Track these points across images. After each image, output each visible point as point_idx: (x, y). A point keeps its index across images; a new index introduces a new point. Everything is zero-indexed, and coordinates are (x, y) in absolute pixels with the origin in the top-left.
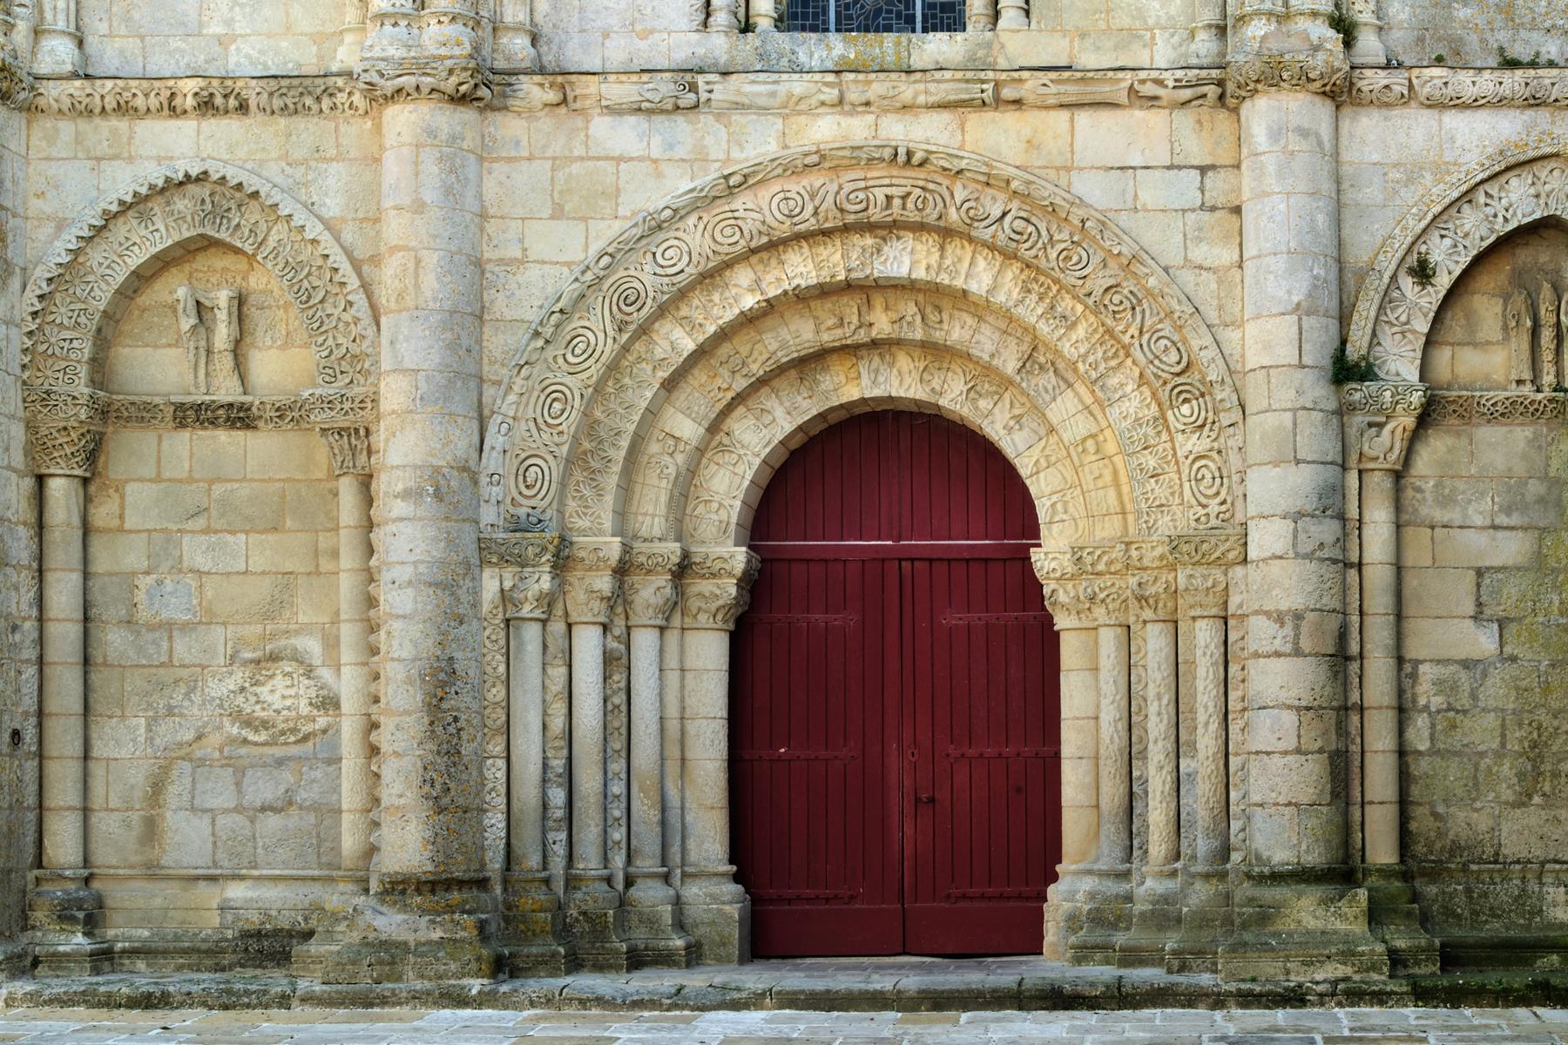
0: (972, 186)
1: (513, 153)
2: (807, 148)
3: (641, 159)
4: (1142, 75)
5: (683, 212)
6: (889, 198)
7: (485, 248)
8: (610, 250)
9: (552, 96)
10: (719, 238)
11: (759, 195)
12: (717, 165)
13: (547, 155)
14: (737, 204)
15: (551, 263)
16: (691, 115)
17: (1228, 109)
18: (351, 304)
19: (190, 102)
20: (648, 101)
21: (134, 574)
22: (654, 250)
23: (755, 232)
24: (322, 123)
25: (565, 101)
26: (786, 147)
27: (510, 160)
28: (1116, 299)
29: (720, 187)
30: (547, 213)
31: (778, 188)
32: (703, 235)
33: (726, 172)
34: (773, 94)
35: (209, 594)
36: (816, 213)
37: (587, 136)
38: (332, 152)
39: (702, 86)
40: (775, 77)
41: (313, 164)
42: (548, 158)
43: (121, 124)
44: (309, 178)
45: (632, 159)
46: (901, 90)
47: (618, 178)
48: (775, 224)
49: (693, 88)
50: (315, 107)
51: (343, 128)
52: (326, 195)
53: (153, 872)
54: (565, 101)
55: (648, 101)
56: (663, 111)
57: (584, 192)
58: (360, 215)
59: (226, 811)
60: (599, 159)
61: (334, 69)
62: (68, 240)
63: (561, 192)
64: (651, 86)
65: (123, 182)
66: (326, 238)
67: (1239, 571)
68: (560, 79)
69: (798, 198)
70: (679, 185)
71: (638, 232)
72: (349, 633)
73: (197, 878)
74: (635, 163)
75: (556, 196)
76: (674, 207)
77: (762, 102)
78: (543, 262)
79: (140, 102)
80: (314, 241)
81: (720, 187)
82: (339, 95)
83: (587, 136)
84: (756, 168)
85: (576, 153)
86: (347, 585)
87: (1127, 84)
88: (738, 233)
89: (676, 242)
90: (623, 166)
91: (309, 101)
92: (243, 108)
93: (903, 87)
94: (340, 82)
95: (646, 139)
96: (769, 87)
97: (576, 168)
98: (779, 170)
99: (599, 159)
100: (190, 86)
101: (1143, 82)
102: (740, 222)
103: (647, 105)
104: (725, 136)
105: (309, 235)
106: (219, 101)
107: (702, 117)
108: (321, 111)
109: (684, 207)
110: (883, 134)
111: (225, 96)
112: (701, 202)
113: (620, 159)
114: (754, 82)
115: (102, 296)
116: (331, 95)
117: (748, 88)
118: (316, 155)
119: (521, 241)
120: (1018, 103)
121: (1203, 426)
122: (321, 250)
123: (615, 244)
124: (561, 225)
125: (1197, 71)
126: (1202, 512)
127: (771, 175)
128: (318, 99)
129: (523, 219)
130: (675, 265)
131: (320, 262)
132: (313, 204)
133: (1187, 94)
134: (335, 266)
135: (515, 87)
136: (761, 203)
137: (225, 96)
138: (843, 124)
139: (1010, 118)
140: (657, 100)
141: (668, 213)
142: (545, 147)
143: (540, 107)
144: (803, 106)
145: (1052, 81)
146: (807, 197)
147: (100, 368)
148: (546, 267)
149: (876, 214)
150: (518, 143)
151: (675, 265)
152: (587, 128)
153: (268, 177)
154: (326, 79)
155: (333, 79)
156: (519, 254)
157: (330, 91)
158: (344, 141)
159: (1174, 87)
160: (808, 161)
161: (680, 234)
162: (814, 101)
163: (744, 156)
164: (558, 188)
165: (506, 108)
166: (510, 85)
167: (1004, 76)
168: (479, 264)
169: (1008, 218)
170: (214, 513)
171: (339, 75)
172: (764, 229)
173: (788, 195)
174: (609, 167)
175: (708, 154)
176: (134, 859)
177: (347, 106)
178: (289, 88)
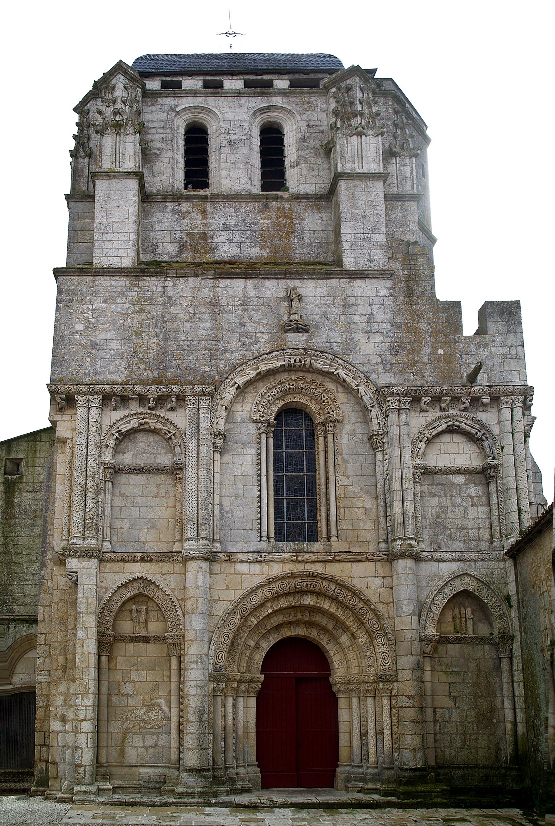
0: (327, 582)
3: (248, 574)
6: (307, 584)
9: (227, 558)
16: (260, 564)
18: (177, 611)
19: (139, 558)
21: (119, 681)
25: (229, 560)
26: (283, 572)
27: (216, 574)
28: (363, 611)
35: (137, 687)
43: (122, 564)
49: (261, 556)
51: (175, 565)
53: (122, 765)
54: (229, 560)
59: (140, 747)
62: (109, 594)
65: (122, 579)
67: (395, 684)
70: (257, 581)
72: (174, 699)
73: (133, 766)
77: (277, 560)
79: (127, 558)
86: (174, 686)
92: (151, 560)
94: (175, 554)
97: (231, 576)
100: (140, 555)
106: (146, 558)
110: (306, 568)
111: (148, 557)
112: (262, 586)
115: (116, 608)
121: (383, 645)
126: (384, 667)
128: (170, 558)
137: (148, 557)
142: (224, 571)
147: (114, 626)
149: (304, 589)
153: (157, 579)
160: (289, 575)
169: (336, 590)
170: (139, 665)
176: (117, 761)
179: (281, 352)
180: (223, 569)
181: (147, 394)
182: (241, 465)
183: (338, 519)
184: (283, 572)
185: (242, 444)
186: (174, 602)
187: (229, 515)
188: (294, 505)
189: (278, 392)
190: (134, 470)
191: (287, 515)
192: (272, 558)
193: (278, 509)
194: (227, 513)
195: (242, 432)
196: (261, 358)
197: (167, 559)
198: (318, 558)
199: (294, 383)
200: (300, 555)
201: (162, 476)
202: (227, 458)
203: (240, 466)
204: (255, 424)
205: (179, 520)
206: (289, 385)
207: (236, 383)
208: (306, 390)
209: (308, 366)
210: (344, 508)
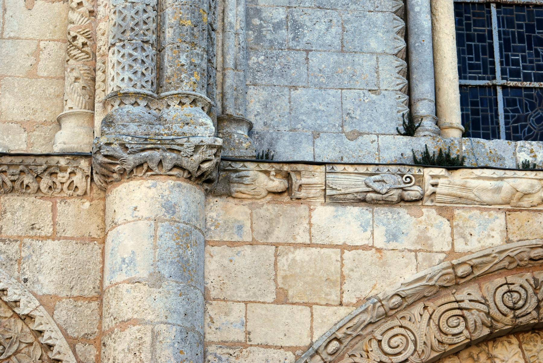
1: (236, 238)
2: (534, 242)
3: (365, 248)
5: (410, 301)
7: (207, 330)
8: (340, 335)
9: (278, 184)
10: (445, 328)
11: (484, 287)
12: (442, 256)
13: (270, 241)
14: (462, 294)
15: (276, 347)
16: (414, 208)
20: (375, 192)
22: (379, 338)
23: (479, 323)
24: (39, 201)
25: (288, 190)
26: (508, 241)
27: (232, 244)
29: (448, 277)
30: (271, 297)
31: (501, 281)
32: (428, 325)
33: (455, 262)
34: (498, 190)
36: (538, 308)
37: (310, 224)
38: (48, 230)
39: (428, 181)
40: (500, 173)
41: (27, 241)
42: (272, 244)
44: (23, 254)
45: (356, 248)
47: (342, 265)
48: (498, 316)
49: (420, 180)
50: (34, 186)
51: (60, 207)
52: (39, 272)
54: (288, 190)
55: (375, 192)
56: (388, 203)
57: (308, 279)
58: (75, 293)
60: (323, 246)
61: (57, 149)
63: (284, 278)
64: (377, 177)
66: (41, 314)
68: (286, 168)
69: (523, 292)
71: (367, 318)
74: (360, 251)
75: (280, 280)
76: (403, 294)
77: (486, 197)
78: (267, 346)
80: (29, 317)
81: (448, 277)
82: (60, 175)
83: (310, 224)
84: (485, 259)
85: (299, 240)
88: (463, 324)
89: (402, 331)
90: (347, 254)
91: (27, 179)
94: (63, 162)
95: (369, 229)
96: (493, 183)
97: (300, 255)
98: (506, 263)
99: (323, 246)
102: (466, 313)
103: (374, 195)
104: (449, 230)
105: (23, 310)
107: (424, 210)
108: (39, 189)
109: (413, 295)
113: (344, 247)
114: (479, 178)
116: (51, 174)
117: (473, 183)
118: (32, 233)
119: (244, 324)
122: (34, 326)
123: (344, 330)
124: (286, 309)
127: (497, 267)
128: (38, 177)
129: (246, 303)
130: (400, 353)
131: (30, 339)
132: (26, 280)
134: (50, 342)
135: (242, 173)
136: (486, 295)
140: (384, 191)
141: (396, 300)
142: (268, 233)
143: (264, 193)
144: (526, 203)
146: (531, 291)
148: (271, 351)
150: (240, 228)
151: (400, 353)
152: (310, 217)
154: (49, 159)
155: (56, 158)
156: (241, 337)
157: (52, 170)
158: (60, 219)
161: (405, 323)
163: (468, 248)
164: (281, 273)
165: (229, 195)
166: (236, 171)
168: (203, 343)
171: (62, 155)
172: (488, 321)
173: (512, 287)
174: (334, 254)
175: (431, 246)
177: (65, 186)
178: (9, 165)
180: (262, 226)
184: (508, 241)
186: (50, 347)
187: (285, 34)
188: (530, 29)
191: (506, 61)
192: (464, 187)
193: (470, 38)
194: (277, 26)
197: (27, 179)
205: (81, 40)
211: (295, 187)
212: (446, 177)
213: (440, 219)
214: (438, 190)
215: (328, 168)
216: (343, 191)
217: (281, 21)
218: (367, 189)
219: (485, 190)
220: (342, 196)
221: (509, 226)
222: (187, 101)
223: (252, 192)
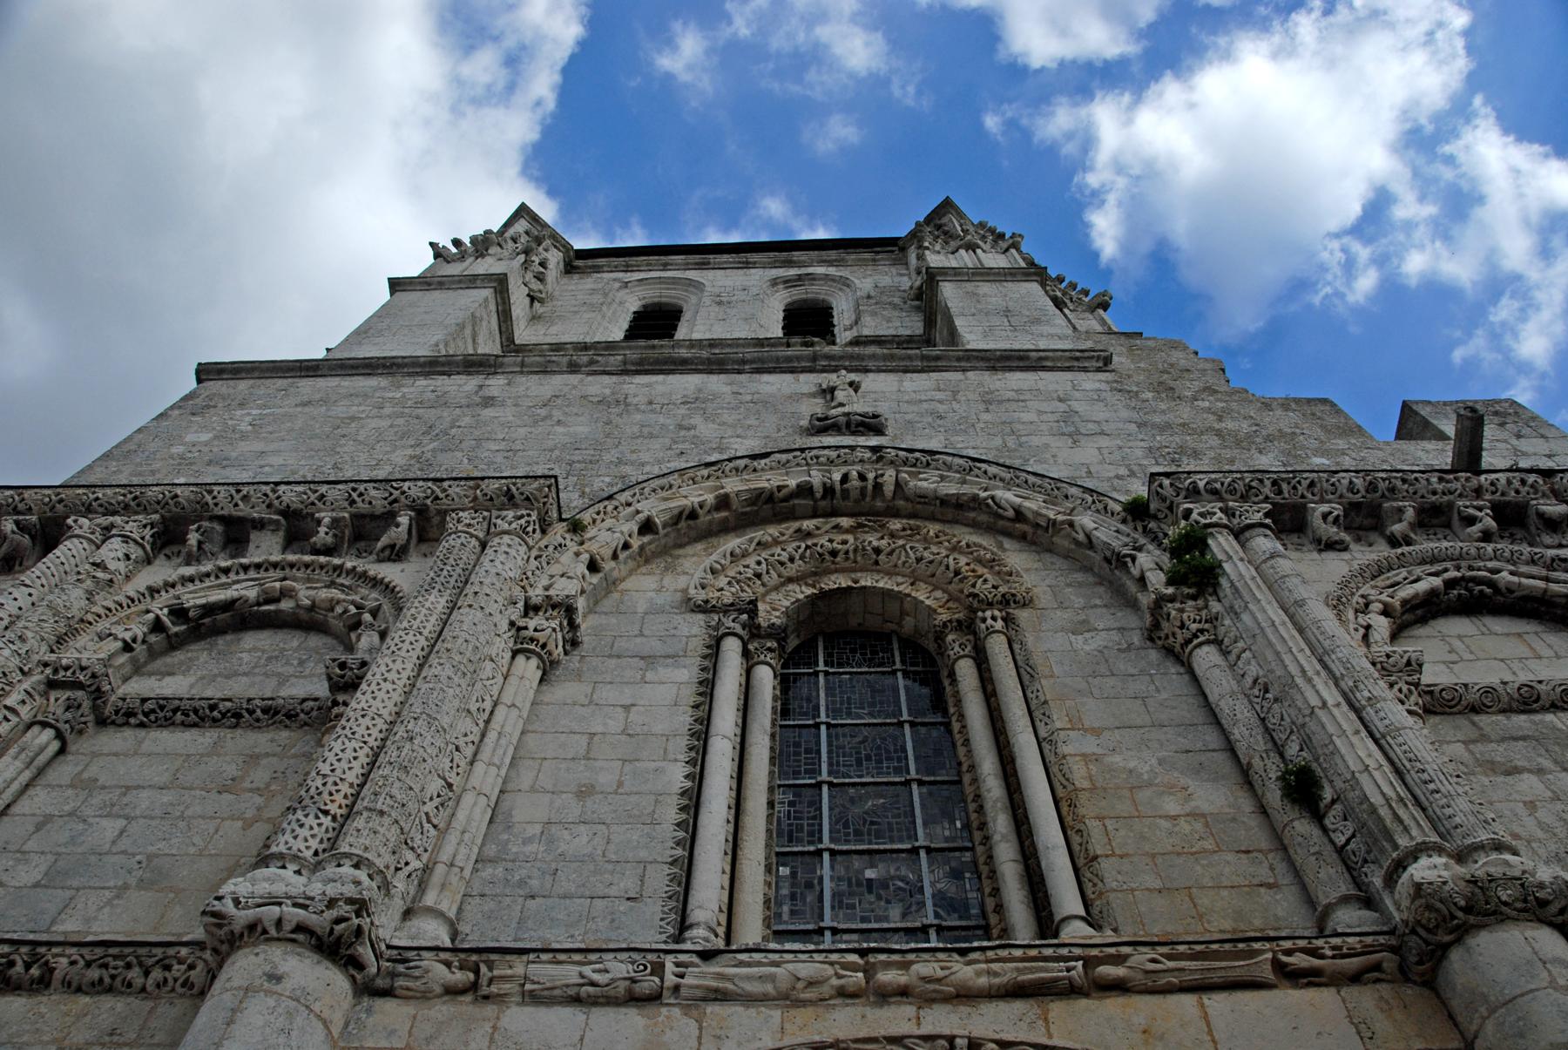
4: (1287, 944)
16: (651, 1009)
17: (1415, 983)
20: (593, 984)
37: (495, 1028)
39: (670, 967)
46: (953, 970)
54: (474, 987)
64: (597, 966)
87: (1269, 955)
91: (135, 974)
93: (956, 967)
94: (184, 951)
101: (1289, 952)
107: (664, 1010)
120: (1119, 987)
125: (1358, 938)
133: (1354, 963)
135: (412, 964)
138: (869, 1015)
139: (1113, 1005)
143: (438, 990)
145: (1161, 955)
157: (167, 962)
159: (1334, 957)
162: (826, 990)
167: (1095, 952)
179: (798, 453)
181: (310, 510)
182: (627, 708)
183: (1081, 862)
185: (642, 658)
189: (792, 560)
190: (175, 711)
192: (721, 977)
195: (646, 632)
196: (731, 465)
198: (989, 973)
199: (850, 538)
200: (887, 965)
201: (285, 734)
202: (564, 690)
203: (620, 710)
204: (701, 616)
206: (831, 541)
207: (638, 512)
208: (891, 553)
209: (889, 489)
210: (1101, 818)
211: (484, 981)
212: (697, 966)
213: (686, 1020)
214: (687, 981)
215: (532, 956)
216: (548, 985)
217: (534, 835)
218: (582, 981)
219: (749, 978)
220: (546, 993)
221: (787, 1026)
222: (348, 862)
223: (423, 988)
